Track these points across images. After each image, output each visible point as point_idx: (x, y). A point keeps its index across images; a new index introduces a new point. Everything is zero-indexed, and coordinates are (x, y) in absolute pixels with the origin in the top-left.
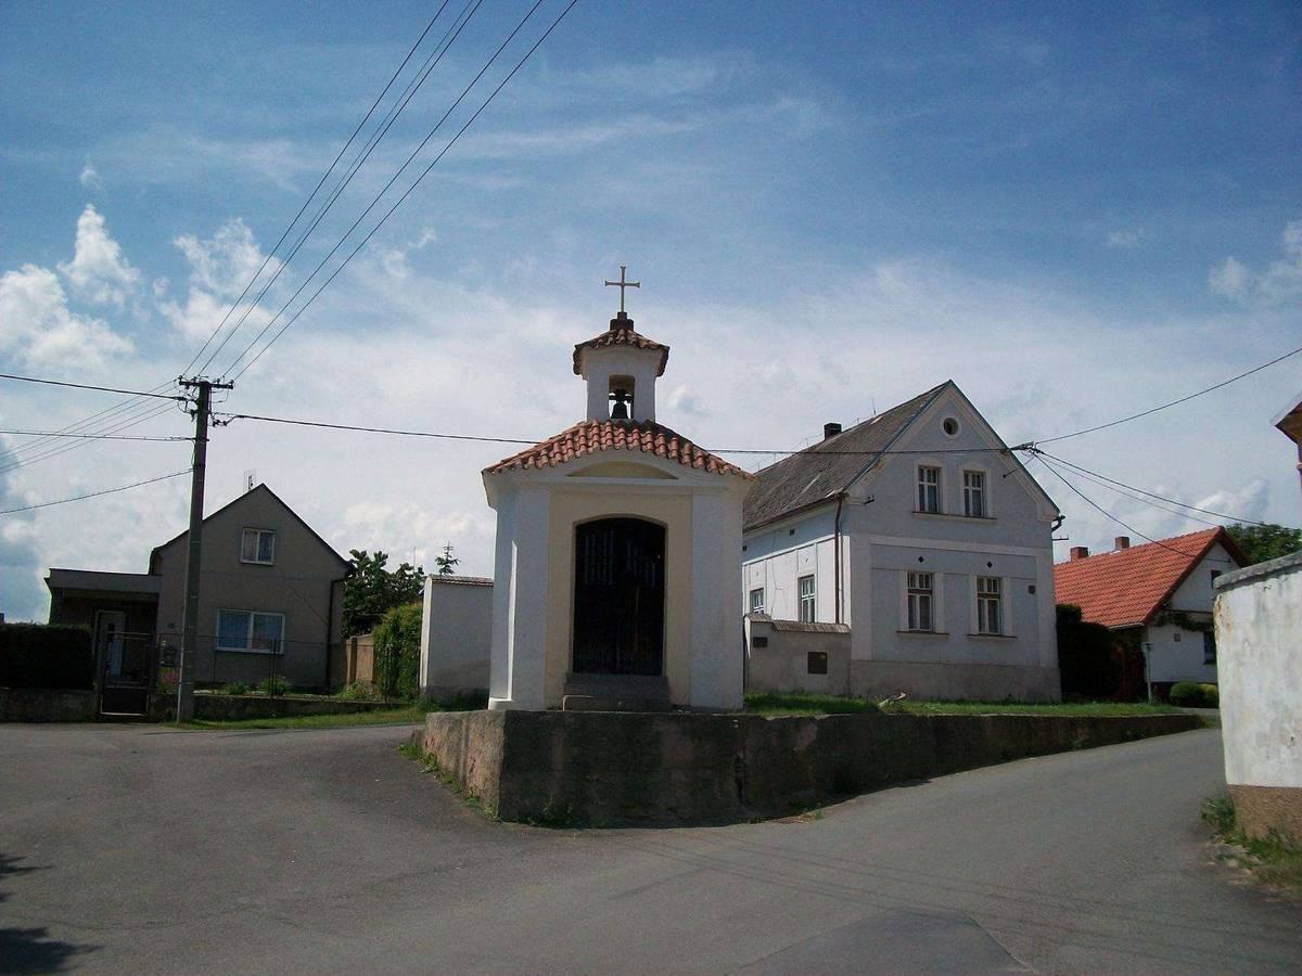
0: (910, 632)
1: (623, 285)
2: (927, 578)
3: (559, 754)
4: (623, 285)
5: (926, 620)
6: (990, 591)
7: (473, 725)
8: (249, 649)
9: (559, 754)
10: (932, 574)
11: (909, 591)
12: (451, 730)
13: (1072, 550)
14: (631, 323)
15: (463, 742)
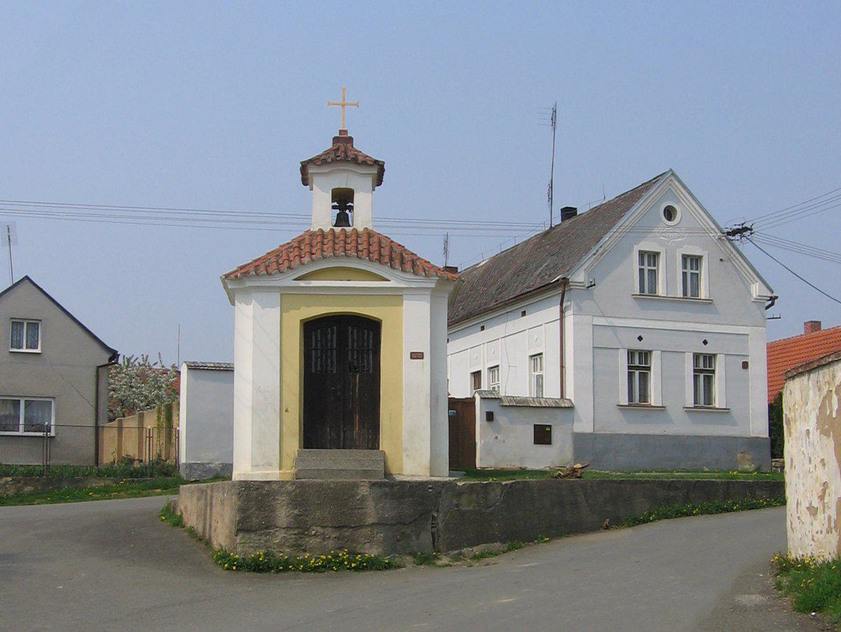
0: (695, 407)
1: (343, 106)
2: (645, 355)
3: (283, 515)
4: (343, 106)
5: (644, 396)
6: (704, 367)
7: (215, 494)
8: (21, 432)
9: (283, 515)
10: (715, 355)
11: (629, 367)
12: (199, 499)
13: (805, 324)
14: (350, 140)
15: (208, 508)
